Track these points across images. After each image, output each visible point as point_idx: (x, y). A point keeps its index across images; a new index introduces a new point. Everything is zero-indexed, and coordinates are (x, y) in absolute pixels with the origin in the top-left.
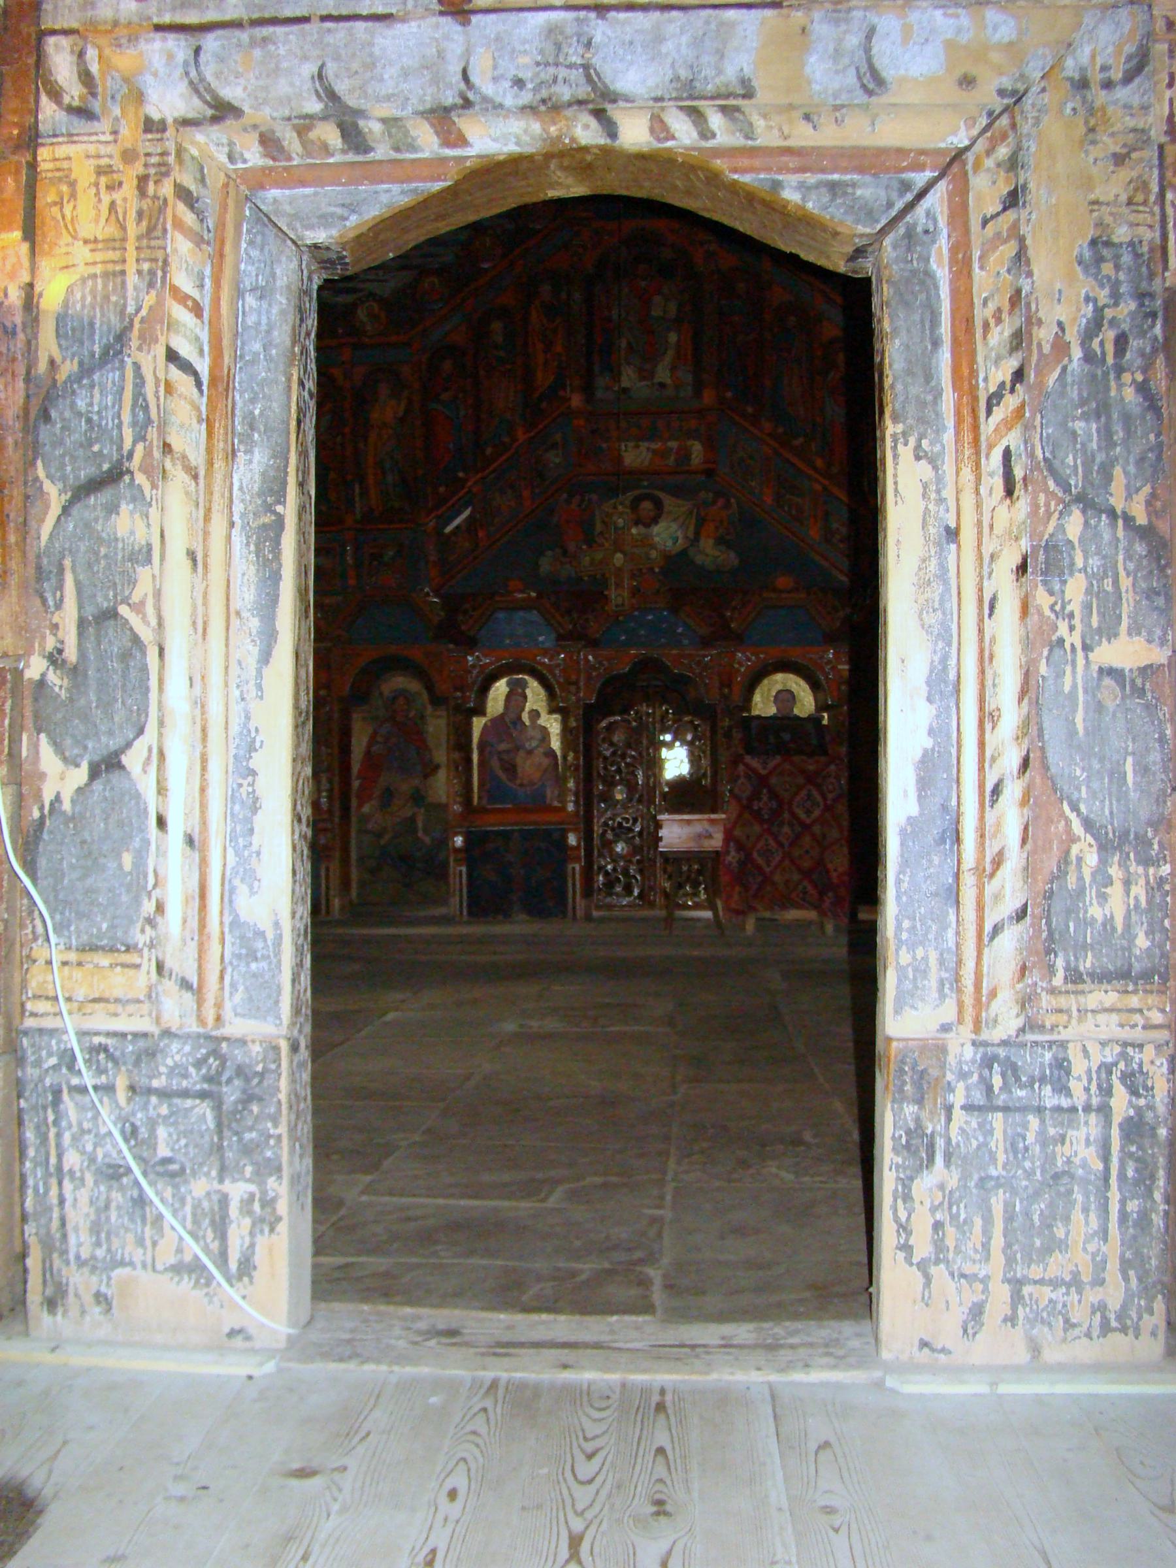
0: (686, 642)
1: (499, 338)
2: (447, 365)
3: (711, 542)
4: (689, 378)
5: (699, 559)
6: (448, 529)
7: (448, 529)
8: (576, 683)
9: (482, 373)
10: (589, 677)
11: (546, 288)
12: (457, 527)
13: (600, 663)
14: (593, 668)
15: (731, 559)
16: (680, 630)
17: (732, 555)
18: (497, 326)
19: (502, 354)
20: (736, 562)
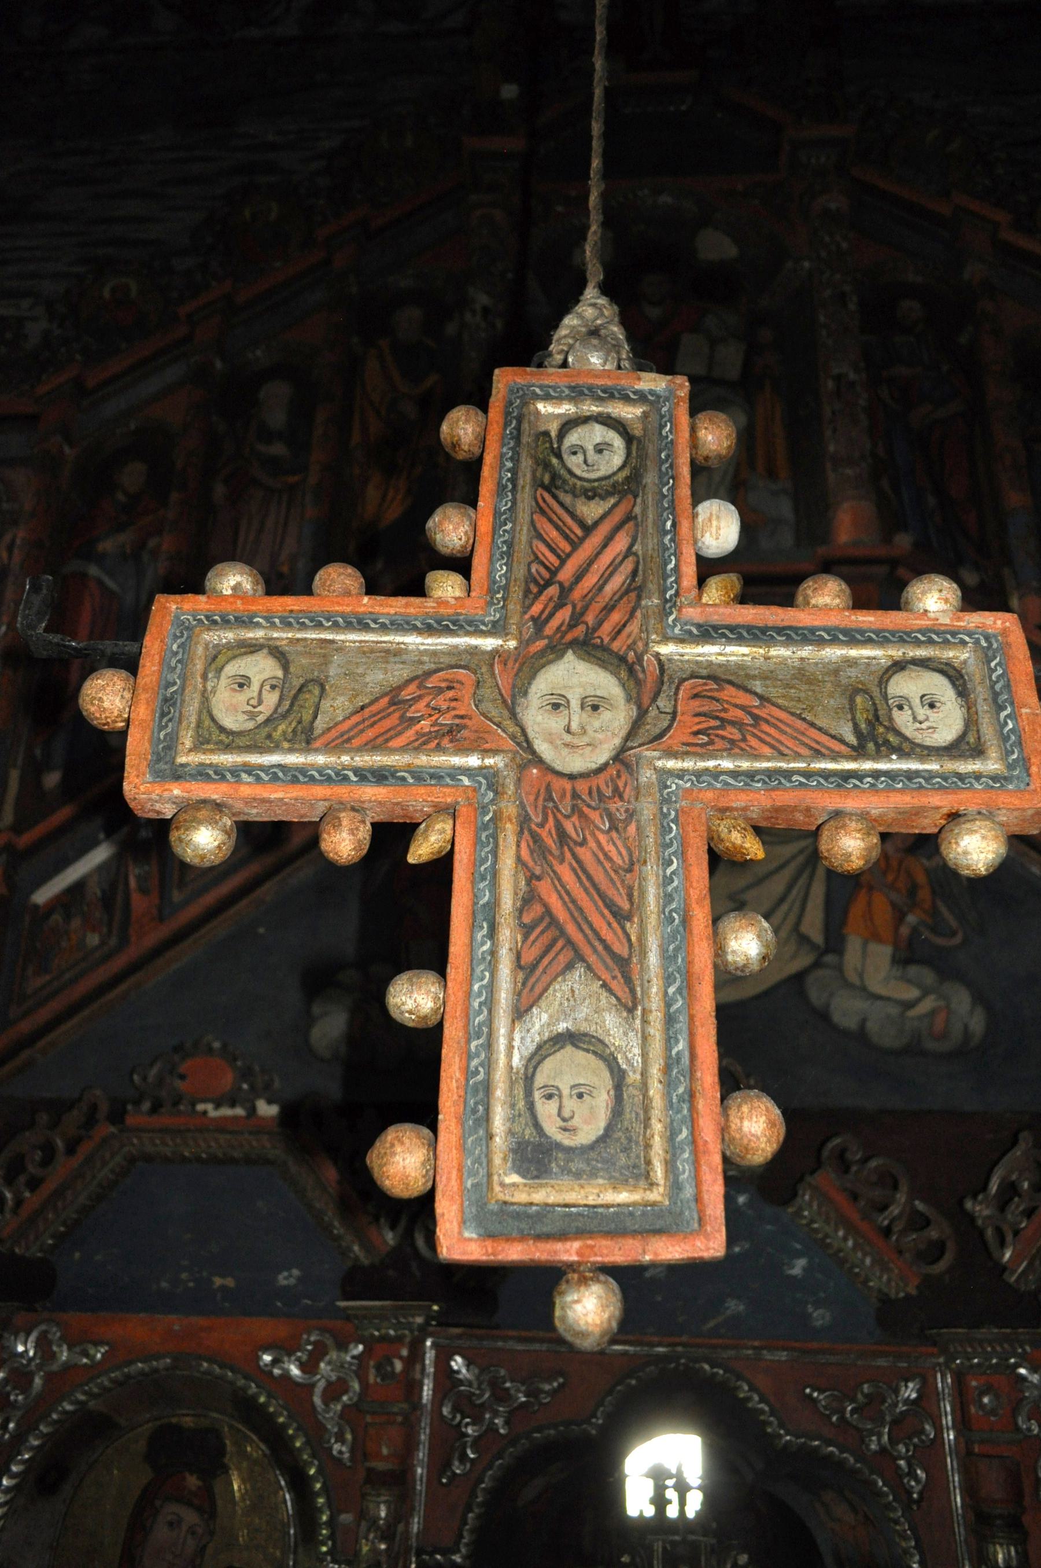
0: (820, 1317)
1: (277, 418)
2: (132, 476)
3: (882, 953)
4: (785, 509)
5: (846, 1011)
6: (42, 896)
7: (42, 896)
8: (398, 1480)
9: (220, 491)
10: (447, 1443)
11: (408, 320)
12: (78, 888)
13: (501, 1396)
14: (467, 1406)
15: (963, 1013)
16: (798, 1267)
17: (961, 1000)
18: (275, 403)
19: (278, 449)
20: (977, 1024)
